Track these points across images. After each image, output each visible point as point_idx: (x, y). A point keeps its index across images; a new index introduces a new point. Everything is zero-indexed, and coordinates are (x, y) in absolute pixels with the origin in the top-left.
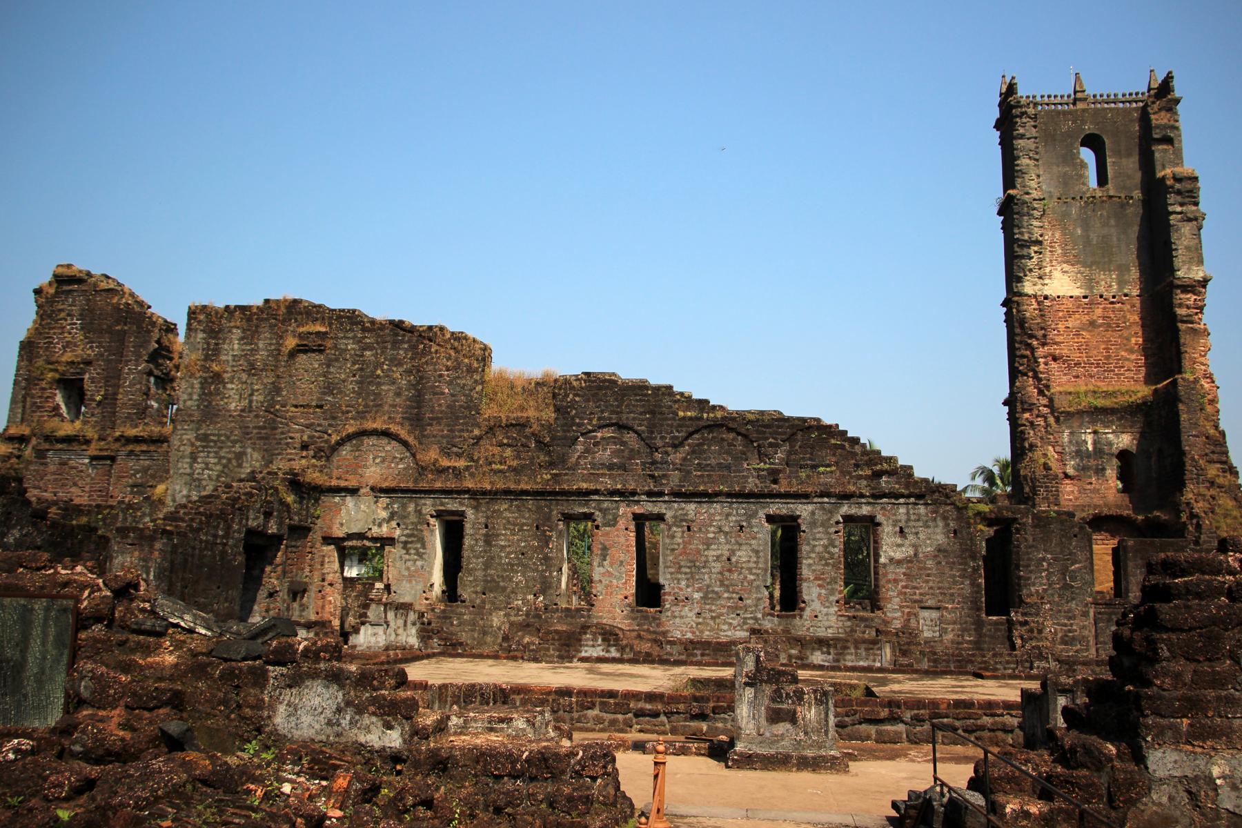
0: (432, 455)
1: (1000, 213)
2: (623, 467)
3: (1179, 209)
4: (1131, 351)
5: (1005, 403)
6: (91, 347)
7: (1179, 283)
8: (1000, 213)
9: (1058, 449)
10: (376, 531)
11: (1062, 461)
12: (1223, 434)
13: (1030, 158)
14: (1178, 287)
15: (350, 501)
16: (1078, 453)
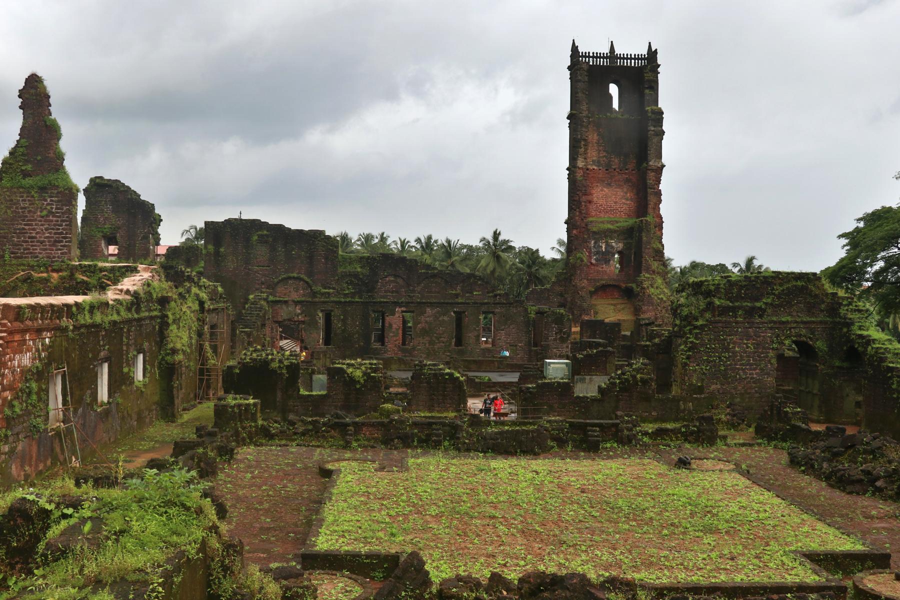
0: (319, 288)
1: (568, 118)
2: (397, 292)
3: (653, 129)
4: (627, 200)
5: (565, 223)
6: (119, 220)
7: (650, 168)
8: (568, 118)
9: (588, 250)
10: (296, 319)
11: (590, 257)
12: (663, 246)
13: (583, 93)
14: (649, 170)
15: (284, 307)
16: (597, 253)
